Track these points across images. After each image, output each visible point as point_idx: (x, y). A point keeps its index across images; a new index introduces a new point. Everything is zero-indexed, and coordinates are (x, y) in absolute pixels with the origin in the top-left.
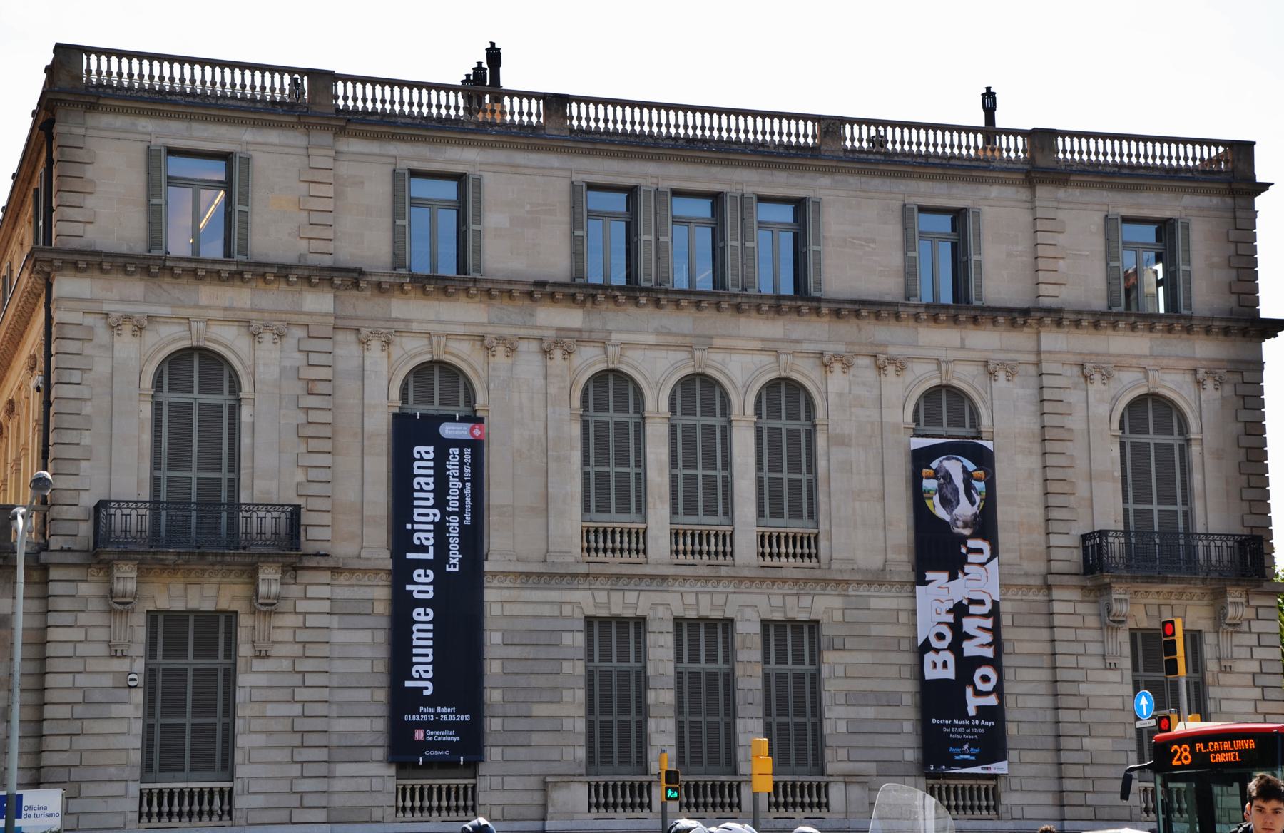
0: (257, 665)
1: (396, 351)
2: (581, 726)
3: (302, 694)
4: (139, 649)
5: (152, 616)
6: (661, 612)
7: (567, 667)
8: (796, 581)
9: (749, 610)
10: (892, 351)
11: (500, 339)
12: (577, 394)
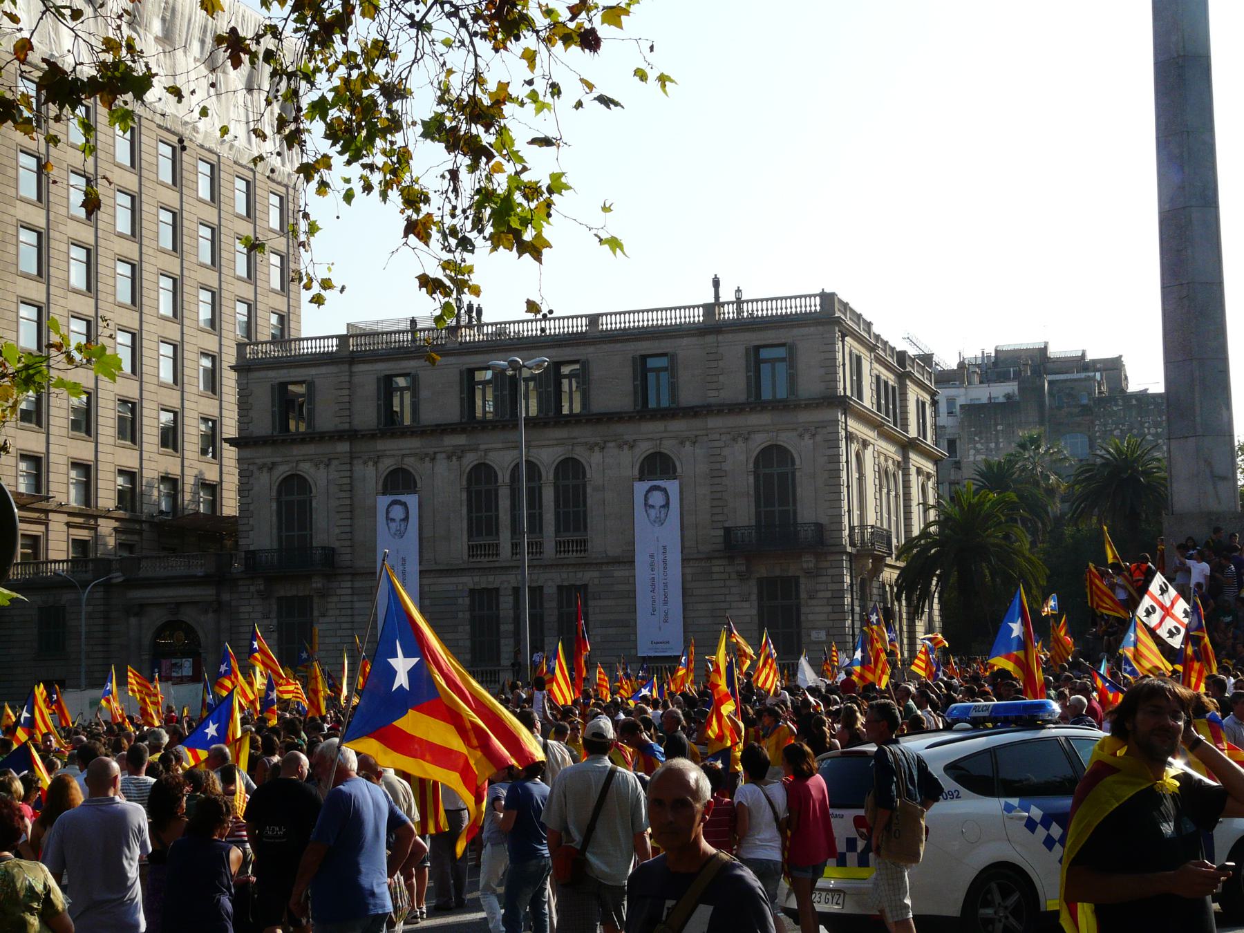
0: (321, 620)
1: (381, 466)
2: (468, 643)
3: (340, 633)
4: (273, 615)
5: (280, 599)
6: (506, 585)
7: (460, 615)
8: (574, 565)
9: (551, 581)
10: (626, 437)
11: (427, 455)
12: (465, 477)
